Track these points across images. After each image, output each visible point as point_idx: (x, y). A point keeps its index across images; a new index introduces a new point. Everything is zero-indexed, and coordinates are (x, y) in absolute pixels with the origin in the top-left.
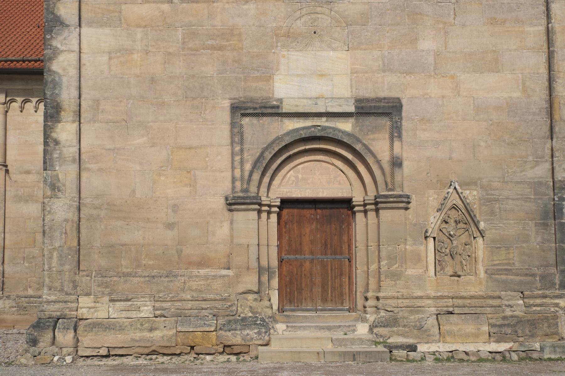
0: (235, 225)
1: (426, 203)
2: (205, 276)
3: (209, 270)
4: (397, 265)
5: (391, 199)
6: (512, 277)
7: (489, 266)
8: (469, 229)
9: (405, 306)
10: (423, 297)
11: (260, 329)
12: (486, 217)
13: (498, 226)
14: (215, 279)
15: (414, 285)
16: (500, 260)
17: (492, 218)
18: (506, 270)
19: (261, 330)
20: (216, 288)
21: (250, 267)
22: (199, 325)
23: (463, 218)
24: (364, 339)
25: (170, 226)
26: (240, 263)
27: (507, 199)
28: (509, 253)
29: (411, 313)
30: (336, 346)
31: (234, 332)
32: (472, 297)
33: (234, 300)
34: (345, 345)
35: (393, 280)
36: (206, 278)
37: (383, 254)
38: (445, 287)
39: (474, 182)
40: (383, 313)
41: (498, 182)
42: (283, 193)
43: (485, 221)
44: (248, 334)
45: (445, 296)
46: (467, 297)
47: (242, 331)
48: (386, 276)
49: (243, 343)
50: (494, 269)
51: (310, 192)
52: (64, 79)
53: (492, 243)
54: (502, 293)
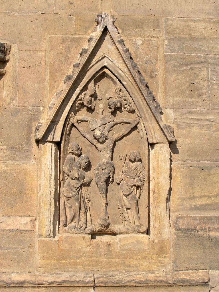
7: (184, 209)
12: (178, 99)
13: (207, 120)
16: (209, 197)
17: (193, 100)
39: (154, 20)
41: (205, 22)
43: (176, 107)
50: (194, 218)
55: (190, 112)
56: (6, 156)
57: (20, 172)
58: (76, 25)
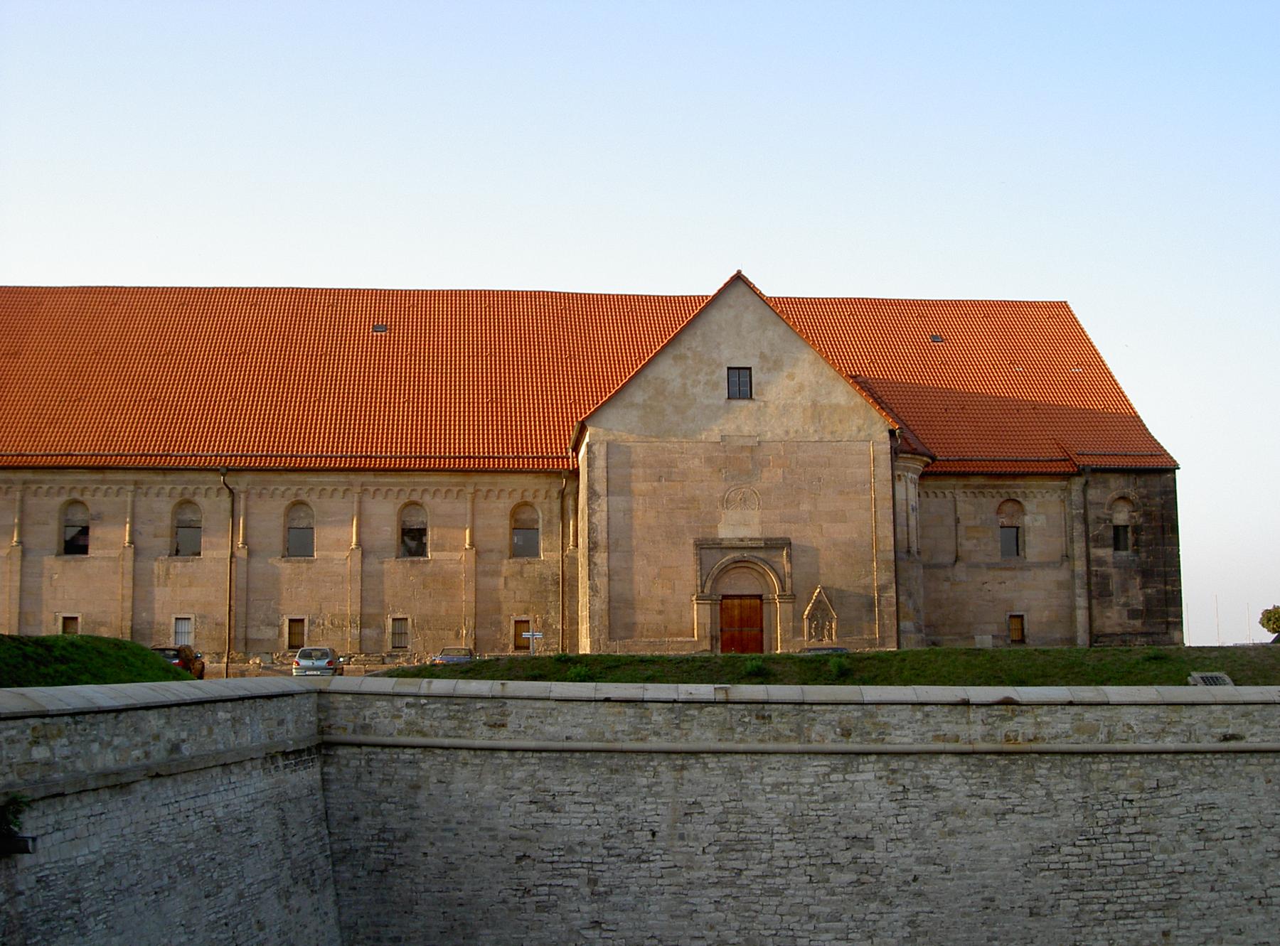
25: (660, 612)
36: (681, 642)
52: (599, 527)
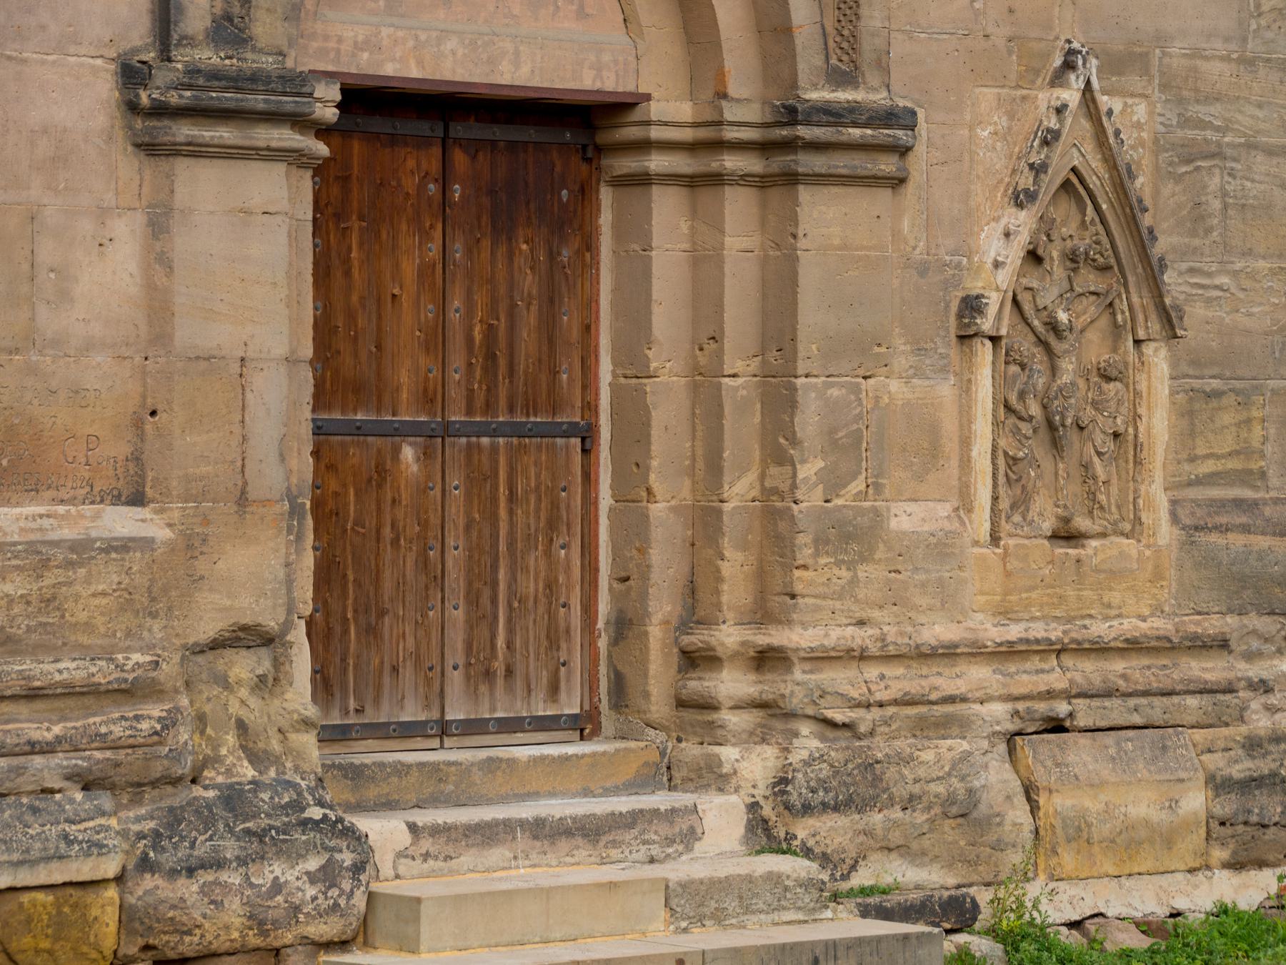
0: (183, 244)
1: (967, 157)
2: (32, 547)
3: (41, 510)
4: (858, 485)
5: (856, 132)
6: (1263, 542)
8: (1117, 301)
9: (899, 695)
10: (956, 646)
11: (332, 850)
13: (1217, 287)
14: (81, 565)
15: (923, 585)
16: (1218, 457)
17: (1197, 242)
18: (1238, 503)
19: (338, 856)
20: (83, 616)
21: (251, 496)
22: (38, 845)
23: (1097, 243)
24: (788, 877)
26: (204, 469)
27: (1251, 146)
28: (1249, 421)
29: (918, 733)
30: (684, 924)
31: (208, 876)
32: (1133, 646)
33: (176, 691)
34: (719, 917)
35: (843, 561)
37: (809, 421)
38: (1034, 595)
39: (1140, 54)
40: (808, 742)
41: (1222, 59)
42: (338, 51)
44: (277, 887)
45: (1037, 641)
46: (1112, 644)
47: (252, 868)
48: (816, 541)
49: (254, 940)
51: (460, 52)
53: (1191, 372)
54: (1229, 619)
55: (1192, 271)
56: (911, 367)
57: (932, 404)
58: (1019, 65)
